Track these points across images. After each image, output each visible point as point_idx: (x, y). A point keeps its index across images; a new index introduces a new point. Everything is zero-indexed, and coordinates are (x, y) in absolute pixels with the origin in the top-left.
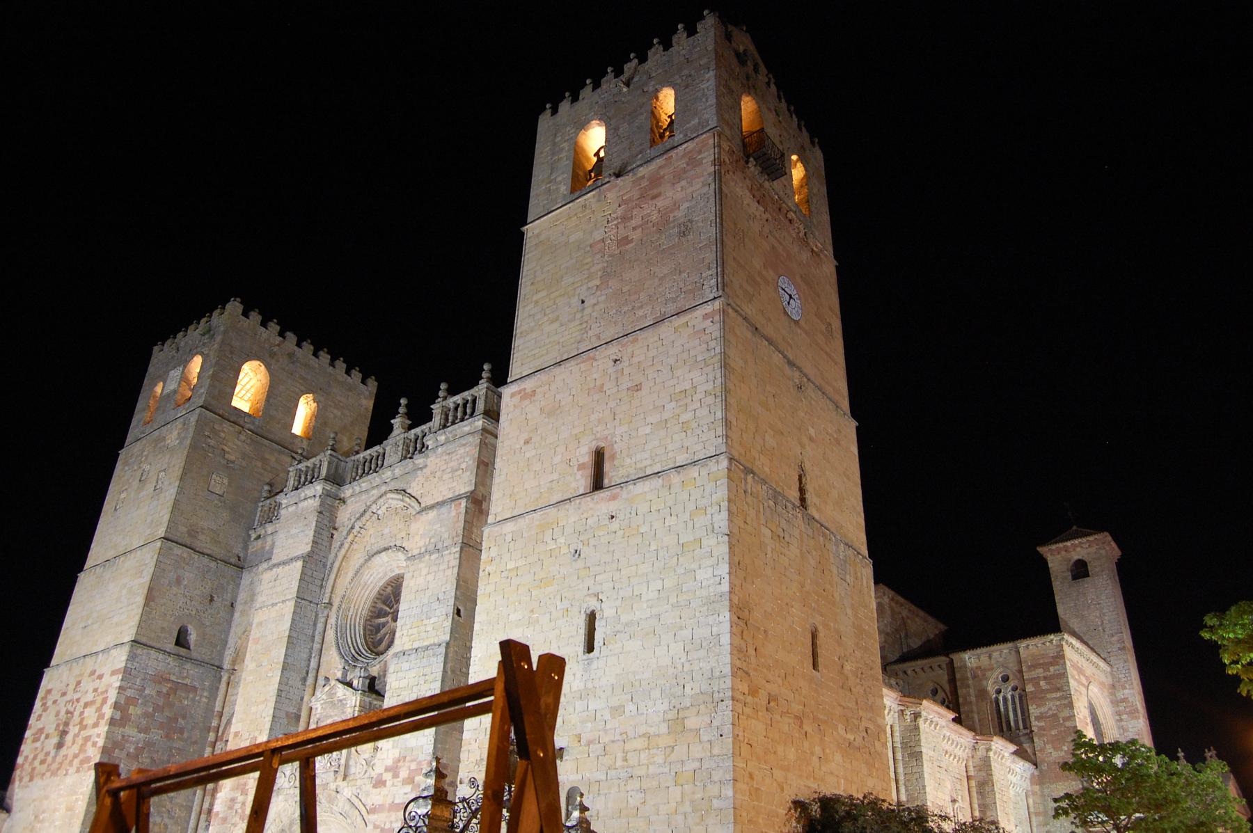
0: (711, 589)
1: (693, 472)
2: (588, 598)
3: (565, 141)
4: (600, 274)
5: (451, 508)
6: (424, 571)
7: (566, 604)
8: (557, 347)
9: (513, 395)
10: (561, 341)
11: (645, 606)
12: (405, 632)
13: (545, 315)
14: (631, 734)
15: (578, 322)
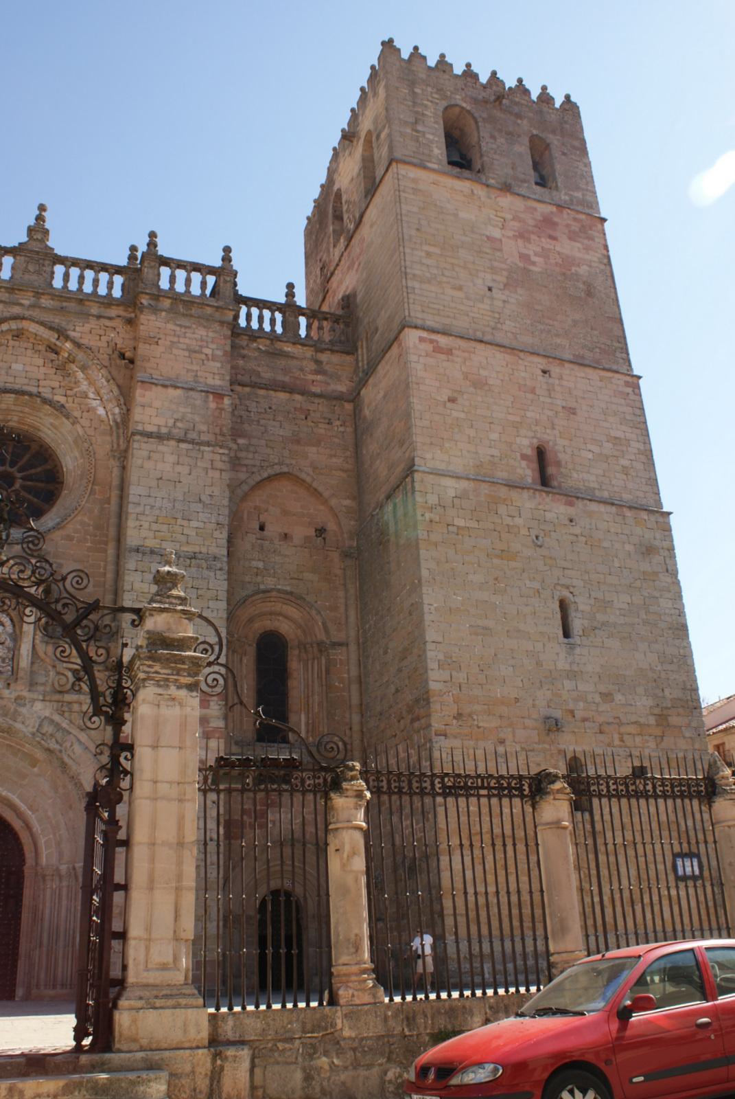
0: (674, 618)
1: (644, 515)
2: (559, 588)
3: (428, 100)
4: (505, 273)
5: (207, 397)
6: (171, 459)
7: (537, 585)
8: (466, 318)
9: (421, 339)
10: (471, 314)
11: (618, 613)
12: (146, 525)
13: (443, 275)
14: (624, 721)
15: (488, 307)
